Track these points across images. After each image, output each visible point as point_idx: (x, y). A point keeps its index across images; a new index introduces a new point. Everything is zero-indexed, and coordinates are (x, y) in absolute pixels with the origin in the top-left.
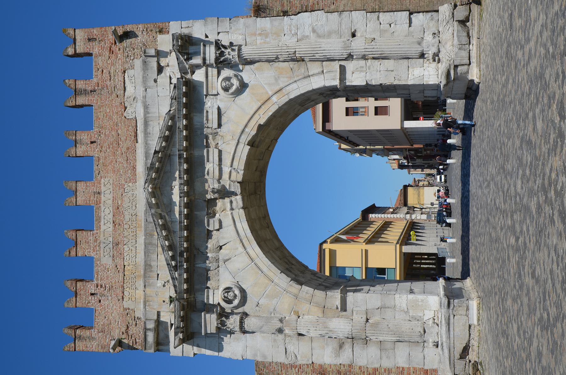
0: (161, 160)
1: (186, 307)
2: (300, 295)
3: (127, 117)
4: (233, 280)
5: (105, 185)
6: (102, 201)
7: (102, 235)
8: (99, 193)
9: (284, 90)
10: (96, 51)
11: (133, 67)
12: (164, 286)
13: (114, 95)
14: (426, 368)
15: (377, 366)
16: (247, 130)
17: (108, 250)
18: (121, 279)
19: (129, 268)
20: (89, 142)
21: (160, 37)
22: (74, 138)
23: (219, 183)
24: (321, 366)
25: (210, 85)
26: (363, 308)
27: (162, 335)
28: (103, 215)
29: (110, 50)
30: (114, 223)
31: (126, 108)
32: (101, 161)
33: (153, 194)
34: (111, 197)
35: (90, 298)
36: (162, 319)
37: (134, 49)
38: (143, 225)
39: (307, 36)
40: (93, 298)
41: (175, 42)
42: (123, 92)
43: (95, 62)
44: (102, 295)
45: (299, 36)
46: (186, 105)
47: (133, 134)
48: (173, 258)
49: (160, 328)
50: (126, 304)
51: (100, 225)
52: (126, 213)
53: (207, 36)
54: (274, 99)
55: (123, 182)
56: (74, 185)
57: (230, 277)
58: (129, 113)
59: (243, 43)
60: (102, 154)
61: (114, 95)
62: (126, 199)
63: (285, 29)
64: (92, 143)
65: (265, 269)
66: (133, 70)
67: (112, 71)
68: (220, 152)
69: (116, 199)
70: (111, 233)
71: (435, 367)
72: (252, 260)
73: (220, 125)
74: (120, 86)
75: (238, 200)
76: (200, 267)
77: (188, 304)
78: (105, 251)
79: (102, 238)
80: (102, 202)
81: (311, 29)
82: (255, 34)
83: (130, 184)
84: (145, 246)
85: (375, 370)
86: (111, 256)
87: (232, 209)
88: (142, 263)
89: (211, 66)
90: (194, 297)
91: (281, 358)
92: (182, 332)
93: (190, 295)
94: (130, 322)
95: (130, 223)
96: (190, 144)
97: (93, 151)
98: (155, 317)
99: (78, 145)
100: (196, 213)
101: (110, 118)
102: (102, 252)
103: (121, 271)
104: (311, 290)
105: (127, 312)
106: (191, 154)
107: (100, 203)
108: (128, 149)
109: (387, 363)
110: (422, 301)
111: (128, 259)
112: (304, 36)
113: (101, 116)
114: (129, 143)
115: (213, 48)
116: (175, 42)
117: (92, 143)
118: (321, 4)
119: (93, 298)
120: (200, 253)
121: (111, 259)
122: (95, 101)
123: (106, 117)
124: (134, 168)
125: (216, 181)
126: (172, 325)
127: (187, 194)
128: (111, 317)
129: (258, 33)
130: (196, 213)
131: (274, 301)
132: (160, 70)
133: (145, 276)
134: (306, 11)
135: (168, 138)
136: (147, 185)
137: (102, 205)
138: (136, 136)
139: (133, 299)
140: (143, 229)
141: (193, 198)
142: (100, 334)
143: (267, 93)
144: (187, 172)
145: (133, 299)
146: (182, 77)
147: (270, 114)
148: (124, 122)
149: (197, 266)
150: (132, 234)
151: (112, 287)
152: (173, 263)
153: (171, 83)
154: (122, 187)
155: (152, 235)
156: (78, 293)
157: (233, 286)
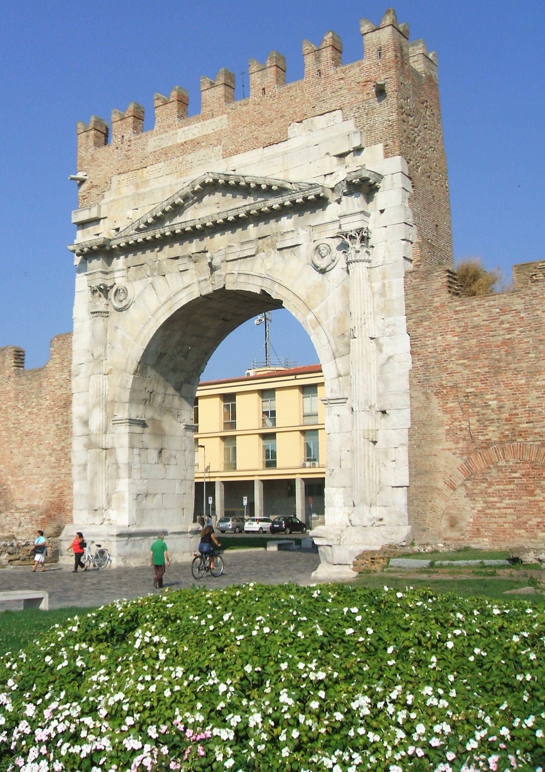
2: (125, 374)
3: (289, 128)
4: (136, 297)
5: (220, 120)
6: (205, 122)
7: (173, 132)
9: (319, 327)
10: (366, 63)
11: (345, 119)
13: (314, 103)
14: (74, 511)
15: (74, 461)
16: (276, 286)
18: (135, 167)
21: (380, 146)
22: (268, 65)
23: (222, 262)
24: (71, 402)
25: (322, 228)
26: (116, 445)
28: (192, 127)
29: (367, 81)
31: (301, 122)
32: (245, 108)
33: (203, 185)
34: (210, 131)
37: (367, 114)
39: (381, 351)
41: (354, 174)
42: (319, 113)
43: (353, 67)
45: (381, 340)
46: (293, 202)
47: (272, 141)
49: (95, 223)
50: (115, 179)
52: (193, 154)
53: (382, 211)
54: (310, 317)
55: (223, 143)
56: (220, 82)
57: (137, 293)
58: (295, 129)
59: (373, 264)
61: (314, 103)
63: (391, 319)
65: (145, 331)
66: (341, 120)
67: (342, 92)
68: (254, 256)
70: (175, 143)
71: (75, 521)
72: (153, 315)
73: (280, 250)
74: (326, 106)
75: (208, 289)
81: (390, 354)
82: (384, 278)
83: (221, 152)
85: (70, 460)
86: (155, 149)
87: (199, 282)
88: (148, 189)
89: (340, 228)
91: (76, 360)
95: (184, 162)
97: (254, 94)
98: (102, 217)
99: (260, 73)
101: (289, 106)
104: (129, 385)
105: (108, 182)
107: (203, 120)
108: (257, 138)
109: (75, 471)
110: (124, 508)
112: (382, 345)
113: (292, 93)
114: (263, 137)
115: (358, 225)
116: (354, 174)
117: (264, 89)
118: (418, 364)
122: (308, 79)
123: (291, 100)
124: (237, 152)
125: (223, 258)
126: (98, 235)
129: (386, 281)
131: (120, 346)
132: (342, 156)
134: (411, 345)
136: (211, 175)
137: (202, 123)
143: (316, 306)
145: (118, 186)
146: (332, 189)
147: (294, 314)
151: (129, 159)
153: (325, 175)
154: (219, 142)
156: (122, 122)
157: (128, 298)
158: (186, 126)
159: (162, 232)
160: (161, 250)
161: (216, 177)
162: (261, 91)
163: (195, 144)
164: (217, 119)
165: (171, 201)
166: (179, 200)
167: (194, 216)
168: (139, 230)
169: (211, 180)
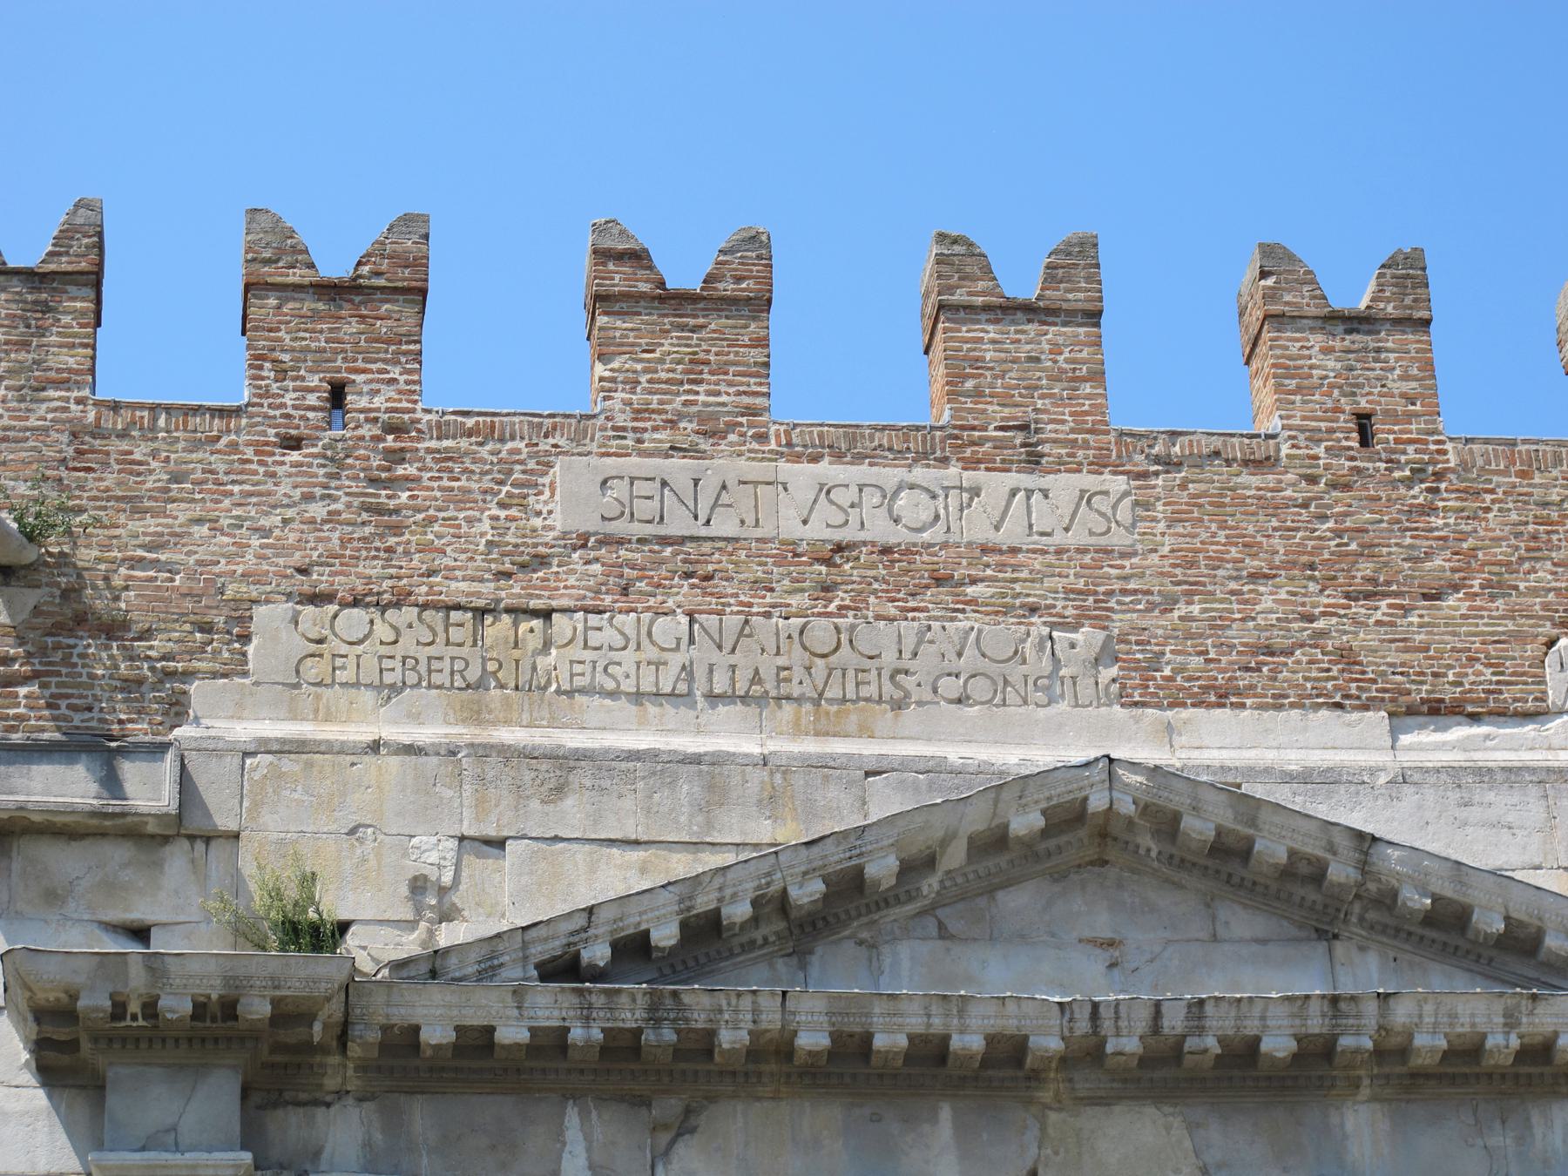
0: (1304, 873)
1: (292, 1036)
5: (1086, 497)
6: (979, 476)
8: (1033, 461)
12: (418, 885)
17: (645, 509)
18: (458, 589)
19: (534, 642)
20: (1363, 404)
27: (65, 861)
28: (891, 475)
30: (839, 548)
33: (1068, 818)
35: (314, 380)
36: (177, 859)
38: (839, 747)
40: (312, 399)
44: (336, 462)
47: (1449, 694)
48: (634, 950)
49: (118, 853)
51: (815, 459)
60: (1291, 487)
62: (1001, 634)
64: (1364, 424)
69: (1001, 567)
76: (559, 1136)
77: (308, 1047)
78: (642, 488)
79: (726, 464)
80: (970, 478)
84: (696, 759)
88: (573, 740)
90: (341, 1094)
92: (119, 1010)
93: (363, 1068)
94: (158, 645)
96: (1419, 1078)
100: (946, 1113)
101: (1536, 549)
102: (634, 464)
103: (512, 592)
106: (1355, 1085)
107: (971, 464)
108: (1346, 657)
111: (595, 638)
117: (1364, 424)
119: (312, 399)
120: (664, 1138)
121: (592, 524)
124: (1223, 696)
126: (140, 933)
127: (1087, 1054)
128: (181, 513)
130: (946, 1113)
133: (482, 751)
135: (1446, 928)
138: (1437, 711)
139: (312, 670)
140: (811, 746)
141: (1046, 1096)
142: (65, 438)
144: (1242, 1055)
145: (312, 670)
148: (1520, 637)
149: (572, 1118)
150: (768, 674)
151: (397, 529)
152: (598, 953)
155: (771, 802)
158: (838, 456)
159: (771, 1019)
160: (684, 1127)
161: (1177, 800)
162: (1345, 421)
163: (926, 577)
164: (1065, 486)
165: (836, 857)
166: (882, 868)
167: (1027, 978)
168: (564, 969)
169: (1126, 807)
